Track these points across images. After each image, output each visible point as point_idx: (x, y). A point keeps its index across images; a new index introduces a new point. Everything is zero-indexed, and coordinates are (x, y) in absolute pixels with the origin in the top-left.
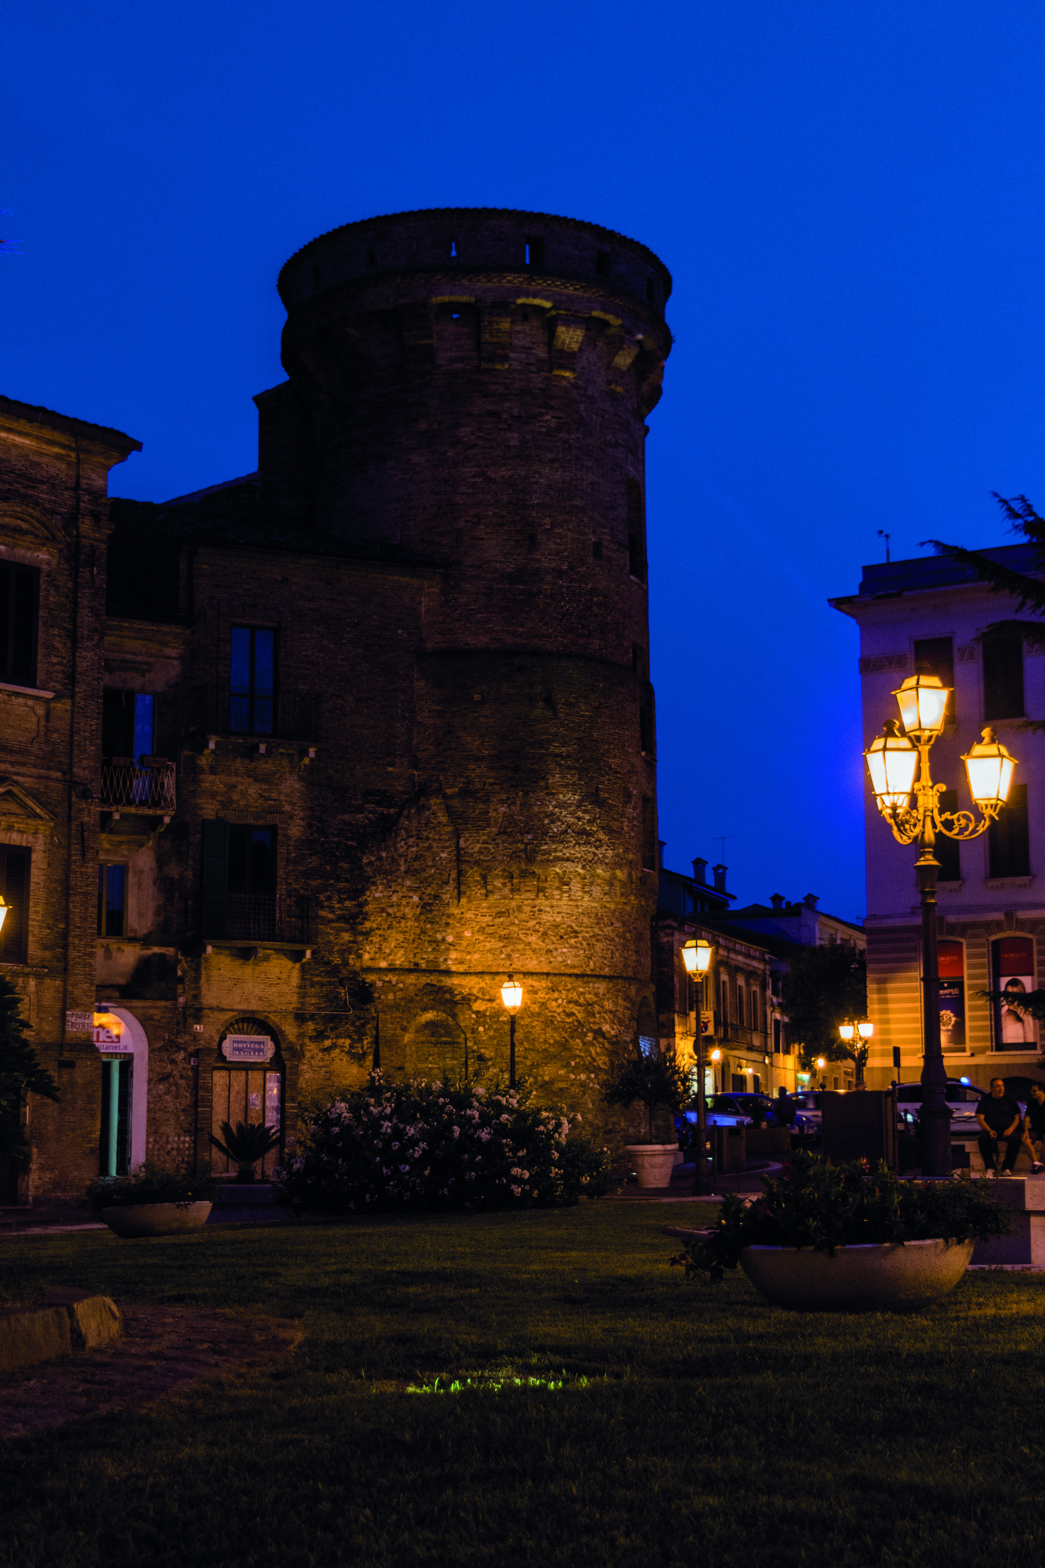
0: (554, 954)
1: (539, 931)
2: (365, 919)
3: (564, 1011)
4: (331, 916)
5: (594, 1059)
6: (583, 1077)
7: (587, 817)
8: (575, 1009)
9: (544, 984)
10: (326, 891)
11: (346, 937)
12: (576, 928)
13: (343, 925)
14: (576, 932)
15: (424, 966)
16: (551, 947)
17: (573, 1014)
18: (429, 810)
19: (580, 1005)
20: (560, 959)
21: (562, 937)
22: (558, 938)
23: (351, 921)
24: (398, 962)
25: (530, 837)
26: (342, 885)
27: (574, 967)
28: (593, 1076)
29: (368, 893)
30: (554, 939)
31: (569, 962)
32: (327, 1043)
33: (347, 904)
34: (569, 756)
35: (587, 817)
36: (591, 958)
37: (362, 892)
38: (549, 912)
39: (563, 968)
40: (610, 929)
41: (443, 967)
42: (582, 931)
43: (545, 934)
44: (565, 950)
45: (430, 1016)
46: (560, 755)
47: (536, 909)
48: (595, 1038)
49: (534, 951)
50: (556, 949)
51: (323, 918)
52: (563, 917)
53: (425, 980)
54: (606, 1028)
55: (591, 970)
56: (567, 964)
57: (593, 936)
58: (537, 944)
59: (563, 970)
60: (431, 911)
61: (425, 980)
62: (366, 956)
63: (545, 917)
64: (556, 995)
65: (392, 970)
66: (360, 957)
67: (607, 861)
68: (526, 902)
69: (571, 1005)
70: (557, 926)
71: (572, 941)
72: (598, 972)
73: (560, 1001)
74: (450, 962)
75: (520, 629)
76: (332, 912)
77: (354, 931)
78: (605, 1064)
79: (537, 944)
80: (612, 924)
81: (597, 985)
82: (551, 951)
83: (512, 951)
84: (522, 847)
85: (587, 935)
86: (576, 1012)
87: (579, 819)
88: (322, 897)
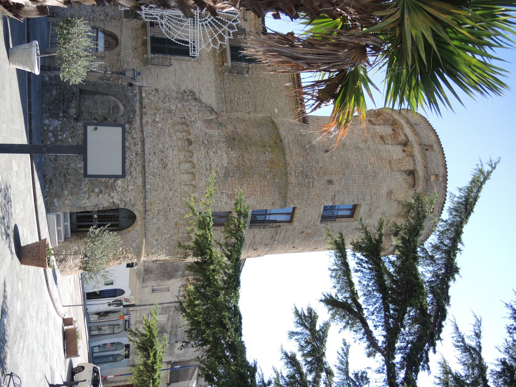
0: (154, 156)
9: (139, 150)
14: (165, 168)
15: (144, 110)
16: (157, 155)
18: (211, 114)
19: (130, 167)
20: (152, 160)
21: (162, 160)
22: (162, 158)
24: (145, 100)
25: (206, 142)
31: (151, 164)
34: (244, 161)
38: (173, 154)
39: (147, 161)
40: (168, 188)
41: (144, 117)
43: (163, 151)
44: (156, 161)
45: (122, 108)
47: (173, 147)
50: (156, 157)
53: (138, 110)
59: (146, 161)
60: (168, 113)
61: (138, 110)
63: (170, 151)
64: (134, 155)
65: (141, 97)
68: (176, 143)
69: (129, 162)
70: (166, 158)
72: (147, 180)
73: (131, 157)
74: (147, 119)
75: (291, 146)
81: (141, 179)
83: (153, 138)
84: (201, 140)
87: (217, 165)
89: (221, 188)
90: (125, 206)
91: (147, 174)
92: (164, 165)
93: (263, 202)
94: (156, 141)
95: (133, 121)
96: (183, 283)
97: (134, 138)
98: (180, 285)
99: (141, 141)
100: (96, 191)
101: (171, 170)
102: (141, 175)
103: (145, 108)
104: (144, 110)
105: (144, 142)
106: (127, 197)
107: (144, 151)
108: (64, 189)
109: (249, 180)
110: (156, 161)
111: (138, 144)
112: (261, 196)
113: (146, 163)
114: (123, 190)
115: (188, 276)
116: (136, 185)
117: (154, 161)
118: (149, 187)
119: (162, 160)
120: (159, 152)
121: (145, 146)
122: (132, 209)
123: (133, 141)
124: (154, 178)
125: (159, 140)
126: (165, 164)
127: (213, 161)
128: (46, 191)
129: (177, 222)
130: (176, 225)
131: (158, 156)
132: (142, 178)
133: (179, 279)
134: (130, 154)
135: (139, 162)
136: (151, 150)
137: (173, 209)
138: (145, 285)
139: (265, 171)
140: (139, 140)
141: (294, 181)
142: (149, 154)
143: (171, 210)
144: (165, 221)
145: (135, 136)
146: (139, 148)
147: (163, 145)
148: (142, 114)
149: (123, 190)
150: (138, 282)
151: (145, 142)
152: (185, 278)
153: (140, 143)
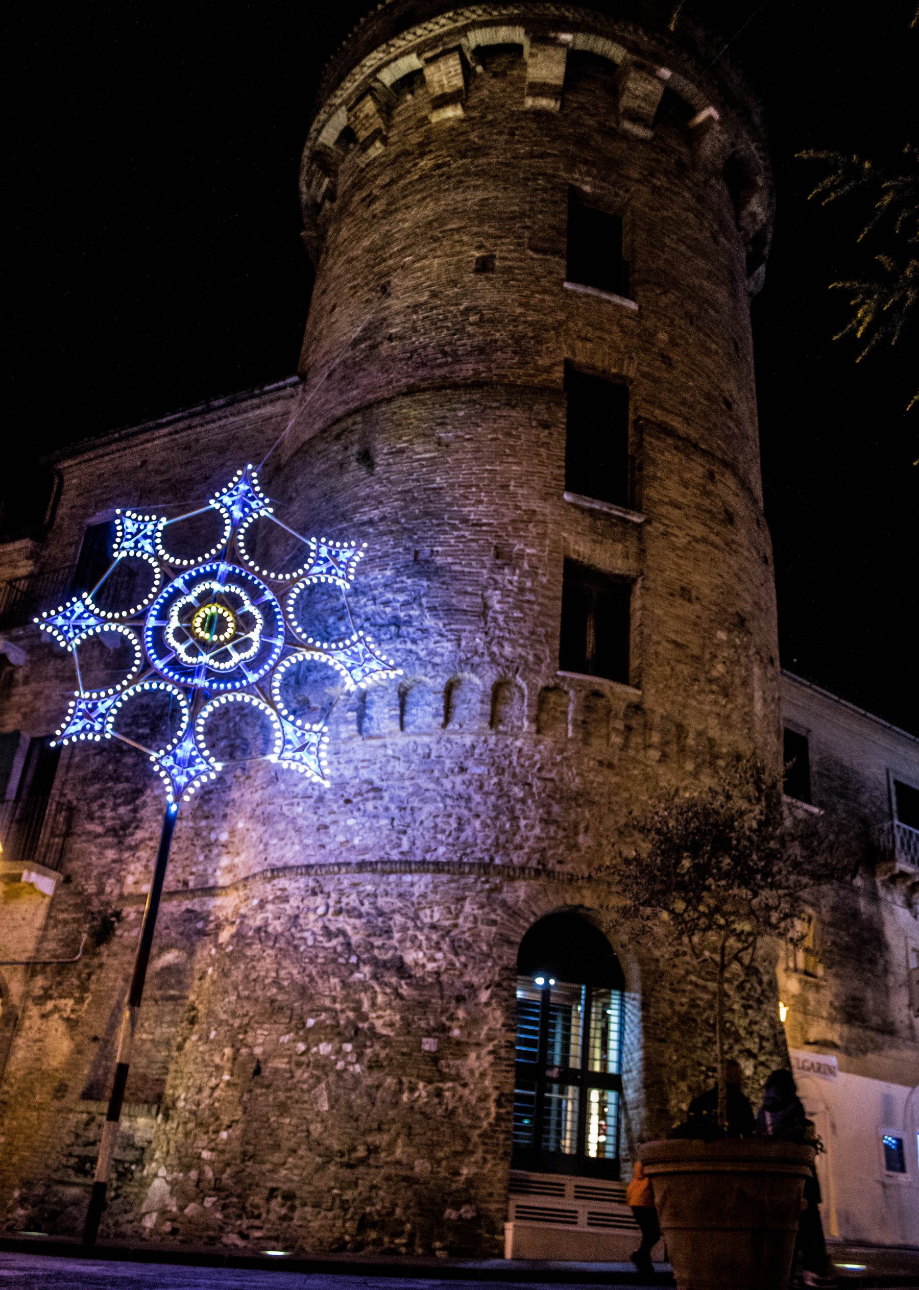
0: (332, 830)
1: (310, 797)
2: (137, 827)
3: (325, 928)
4: (99, 829)
5: (364, 1017)
6: (325, 1048)
7: (401, 598)
8: (344, 923)
9: (302, 882)
10: (101, 797)
11: (111, 854)
12: (378, 783)
13: (110, 839)
14: (378, 790)
16: (327, 820)
17: (341, 932)
19: (360, 916)
21: (348, 801)
22: (341, 802)
23: (121, 833)
26: (120, 786)
27: (366, 850)
28: (348, 1047)
29: (148, 792)
30: (335, 807)
31: (356, 841)
32: (50, 1005)
33: (122, 810)
35: (401, 598)
36: (405, 832)
37: (139, 792)
40: (458, 779)
42: (388, 787)
43: (321, 799)
44: (351, 822)
46: (371, 522)
48: (375, 977)
49: (298, 830)
50: (335, 822)
51: (89, 833)
52: (356, 768)
54: (411, 957)
55: (402, 853)
56: (354, 847)
57: (412, 794)
58: (306, 818)
59: (345, 857)
60: (210, 799)
62: (130, 879)
64: (319, 900)
66: (120, 881)
67: (437, 660)
71: (370, 806)
76: (102, 823)
77: (120, 845)
78: (391, 1025)
79: (306, 818)
80: (463, 770)
81: (408, 878)
82: (326, 827)
83: (271, 836)
85: (403, 794)
86: (349, 929)
87: (386, 603)
88: (95, 806)
89: (469, 589)
90: (510, 943)
91: (395, 855)
92: (368, 791)
93: (538, 455)
94: (281, 826)
95: (217, 918)
96: (899, 903)
97: (262, 905)
98: (907, 911)
99: (273, 878)
100: (434, 1049)
101: (389, 769)
102: (393, 878)
103: (186, 883)
104: (191, 884)
105: (278, 869)
106: (476, 936)
107: (309, 867)
108: (408, 1173)
109: (448, 499)
110: (351, 822)
111: (283, 890)
112: (510, 459)
113: (354, 858)
114: (445, 946)
115: (874, 884)
116: (431, 897)
117: (348, 829)
118: (442, 850)
119: (348, 801)
120: (321, 812)
121: (292, 863)
122: (527, 920)
123: (270, 907)
124: (409, 831)
125: (282, 814)
126: (365, 787)
127: (367, 619)
128: (403, 1250)
129: (601, 763)
130: (610, 766)
131: (333, 817)
132: (405, 872)
133: (885, 914)
134: (312, 917)
135: (346, 883)
136: (309, 841)
137: (540, 770)
138: (906, 1033)
139: (426, 452)
140: (269, 887)
141: (470, 366)
142: (323, 846)
143: (544, 774)
144: (593, 803)
145: (255, 902)
146: (293, 885)
147: (296, 800)
148: (202, 889)
149: (445, 946)
150: (893, 1053)
151: (279, 864)
152: (882, 892)
153: (282, 882)
